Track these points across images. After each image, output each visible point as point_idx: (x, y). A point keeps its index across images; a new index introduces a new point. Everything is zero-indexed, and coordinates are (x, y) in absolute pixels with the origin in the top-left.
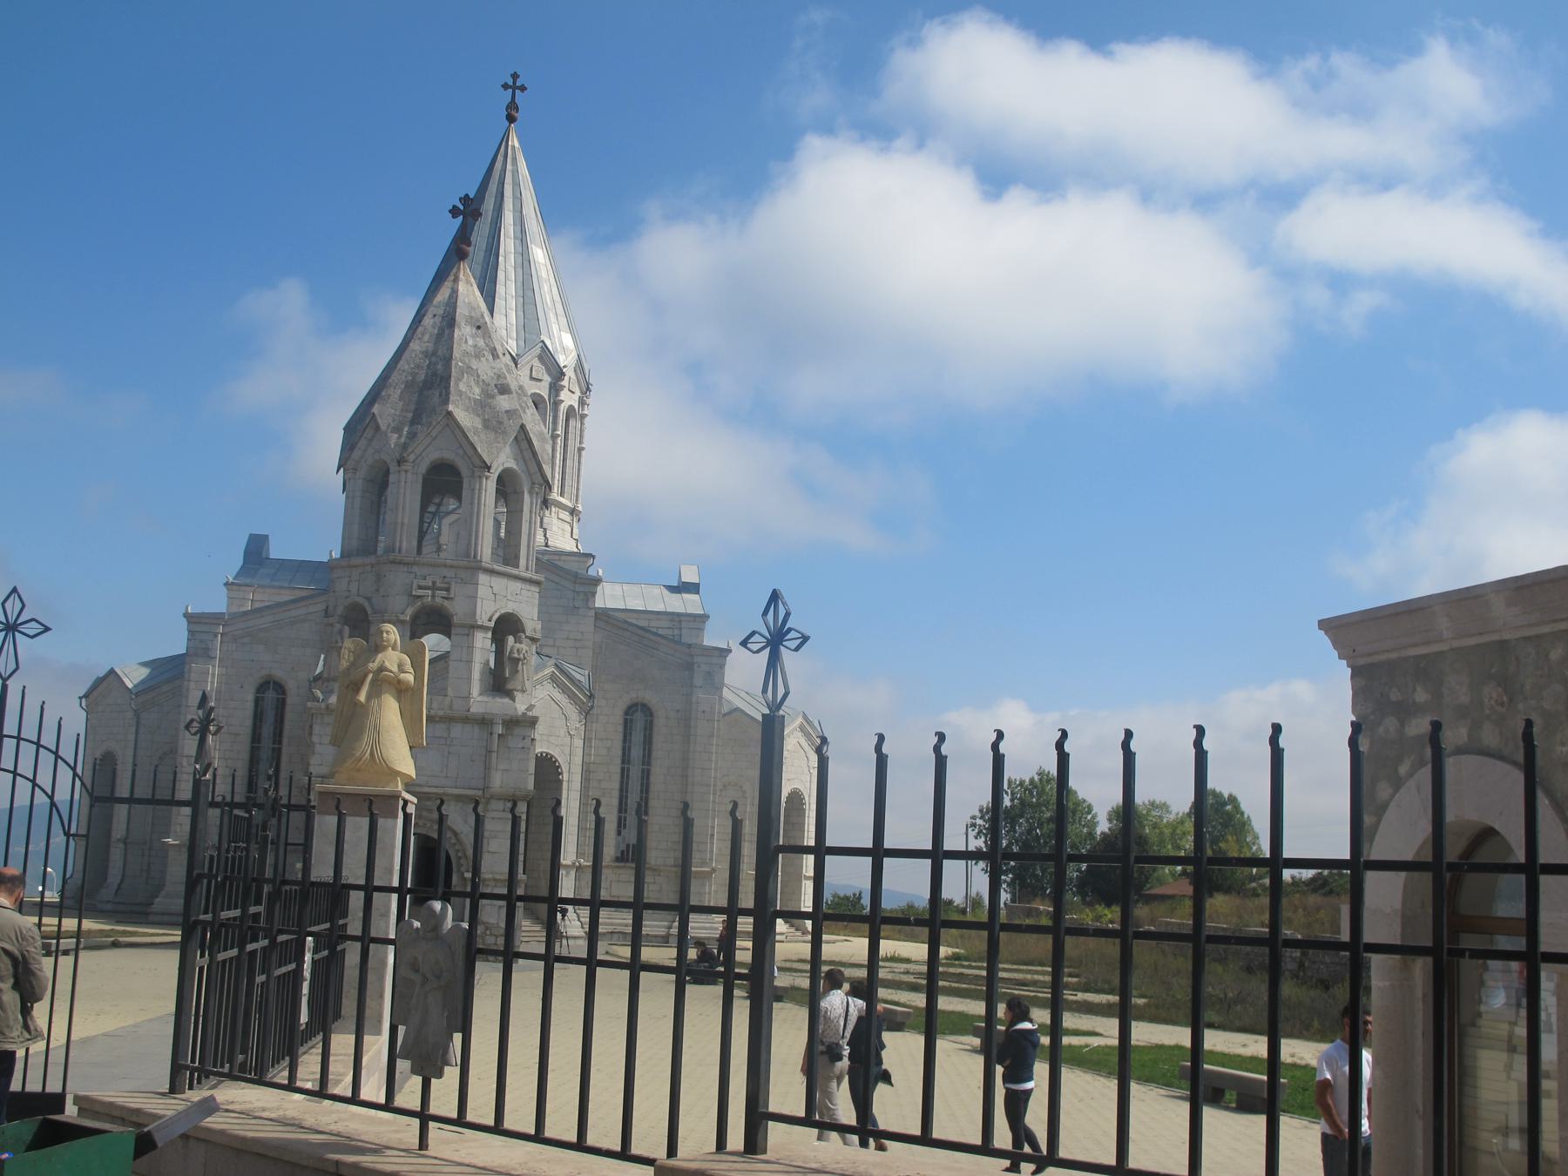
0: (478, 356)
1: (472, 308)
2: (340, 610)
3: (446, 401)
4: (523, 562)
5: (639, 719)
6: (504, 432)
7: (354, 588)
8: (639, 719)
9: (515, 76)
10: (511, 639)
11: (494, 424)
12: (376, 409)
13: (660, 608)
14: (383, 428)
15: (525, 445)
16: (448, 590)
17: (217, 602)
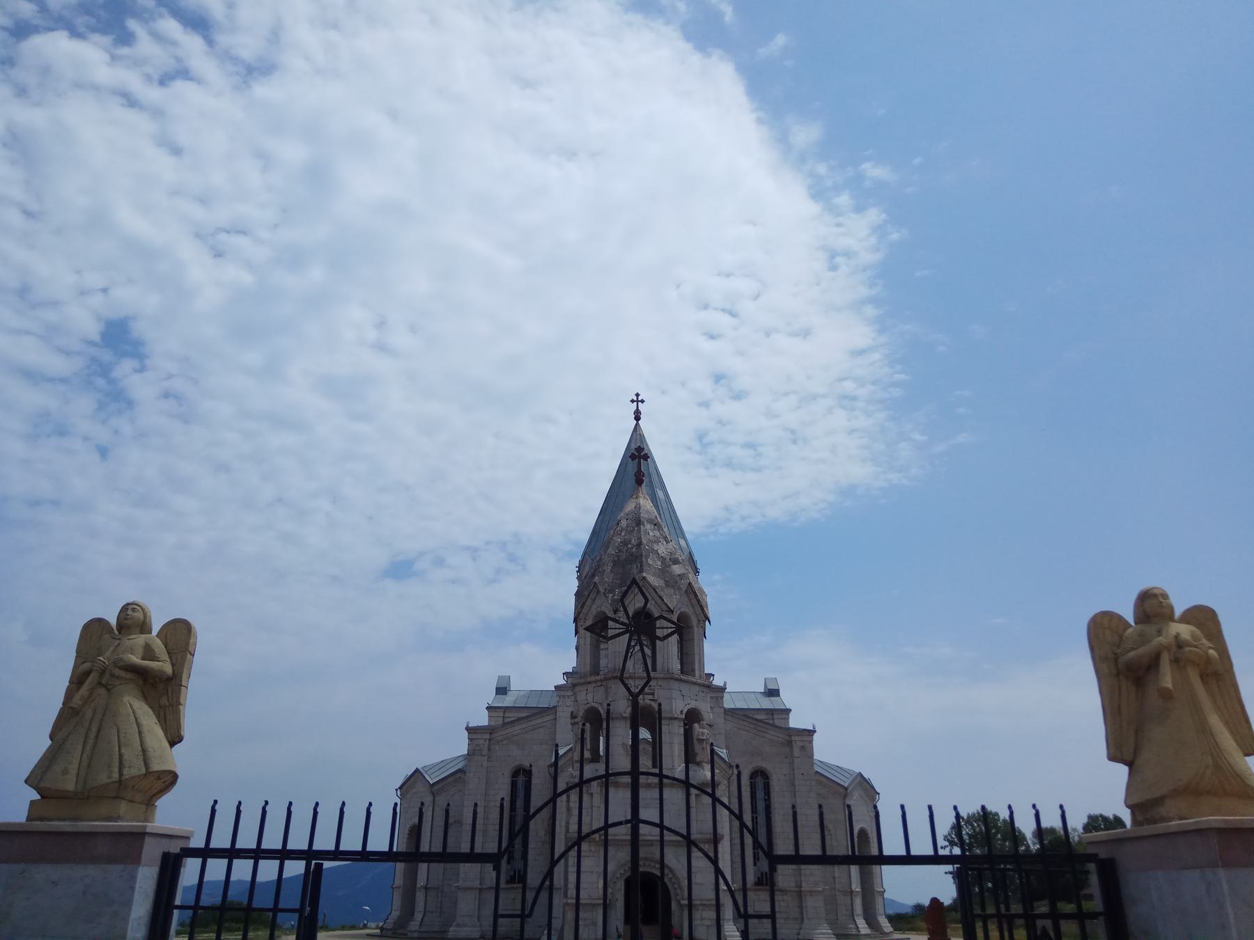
0: (657, 542)
1: (648, 512)
2: (581, 713)
3: (641, 571)
4: (697, 673)
5: (760, 781)
6: (679, 589)
7: (590, 700)
8: (760, 781)
9: (637, 395)
10: (696, 725)
11: (672, 582)
12: (596, 579)
13: (757, 706)
14: (602, 590)
15: (692, 596)
16: (653, 694)
17: (482, 720)
